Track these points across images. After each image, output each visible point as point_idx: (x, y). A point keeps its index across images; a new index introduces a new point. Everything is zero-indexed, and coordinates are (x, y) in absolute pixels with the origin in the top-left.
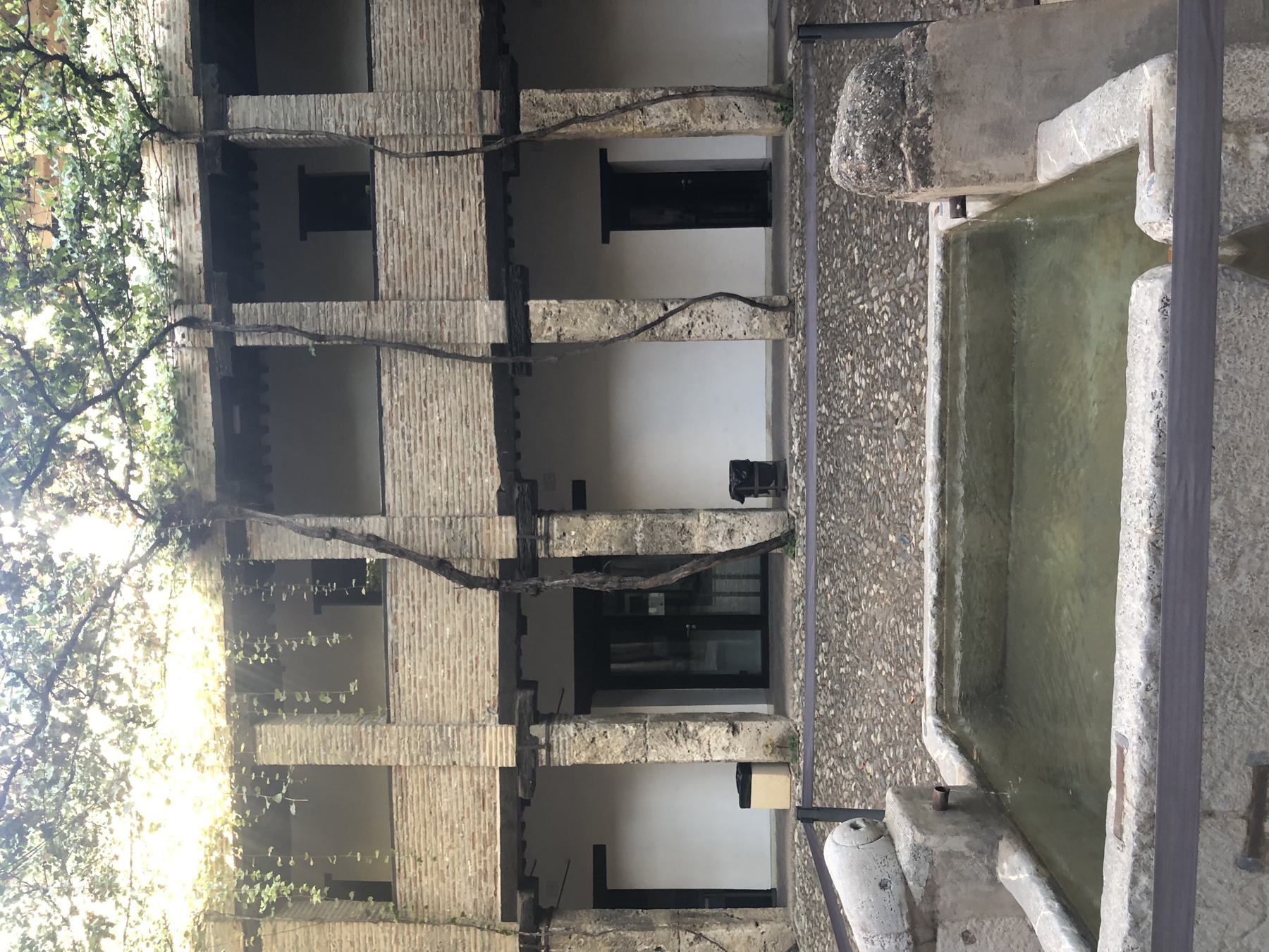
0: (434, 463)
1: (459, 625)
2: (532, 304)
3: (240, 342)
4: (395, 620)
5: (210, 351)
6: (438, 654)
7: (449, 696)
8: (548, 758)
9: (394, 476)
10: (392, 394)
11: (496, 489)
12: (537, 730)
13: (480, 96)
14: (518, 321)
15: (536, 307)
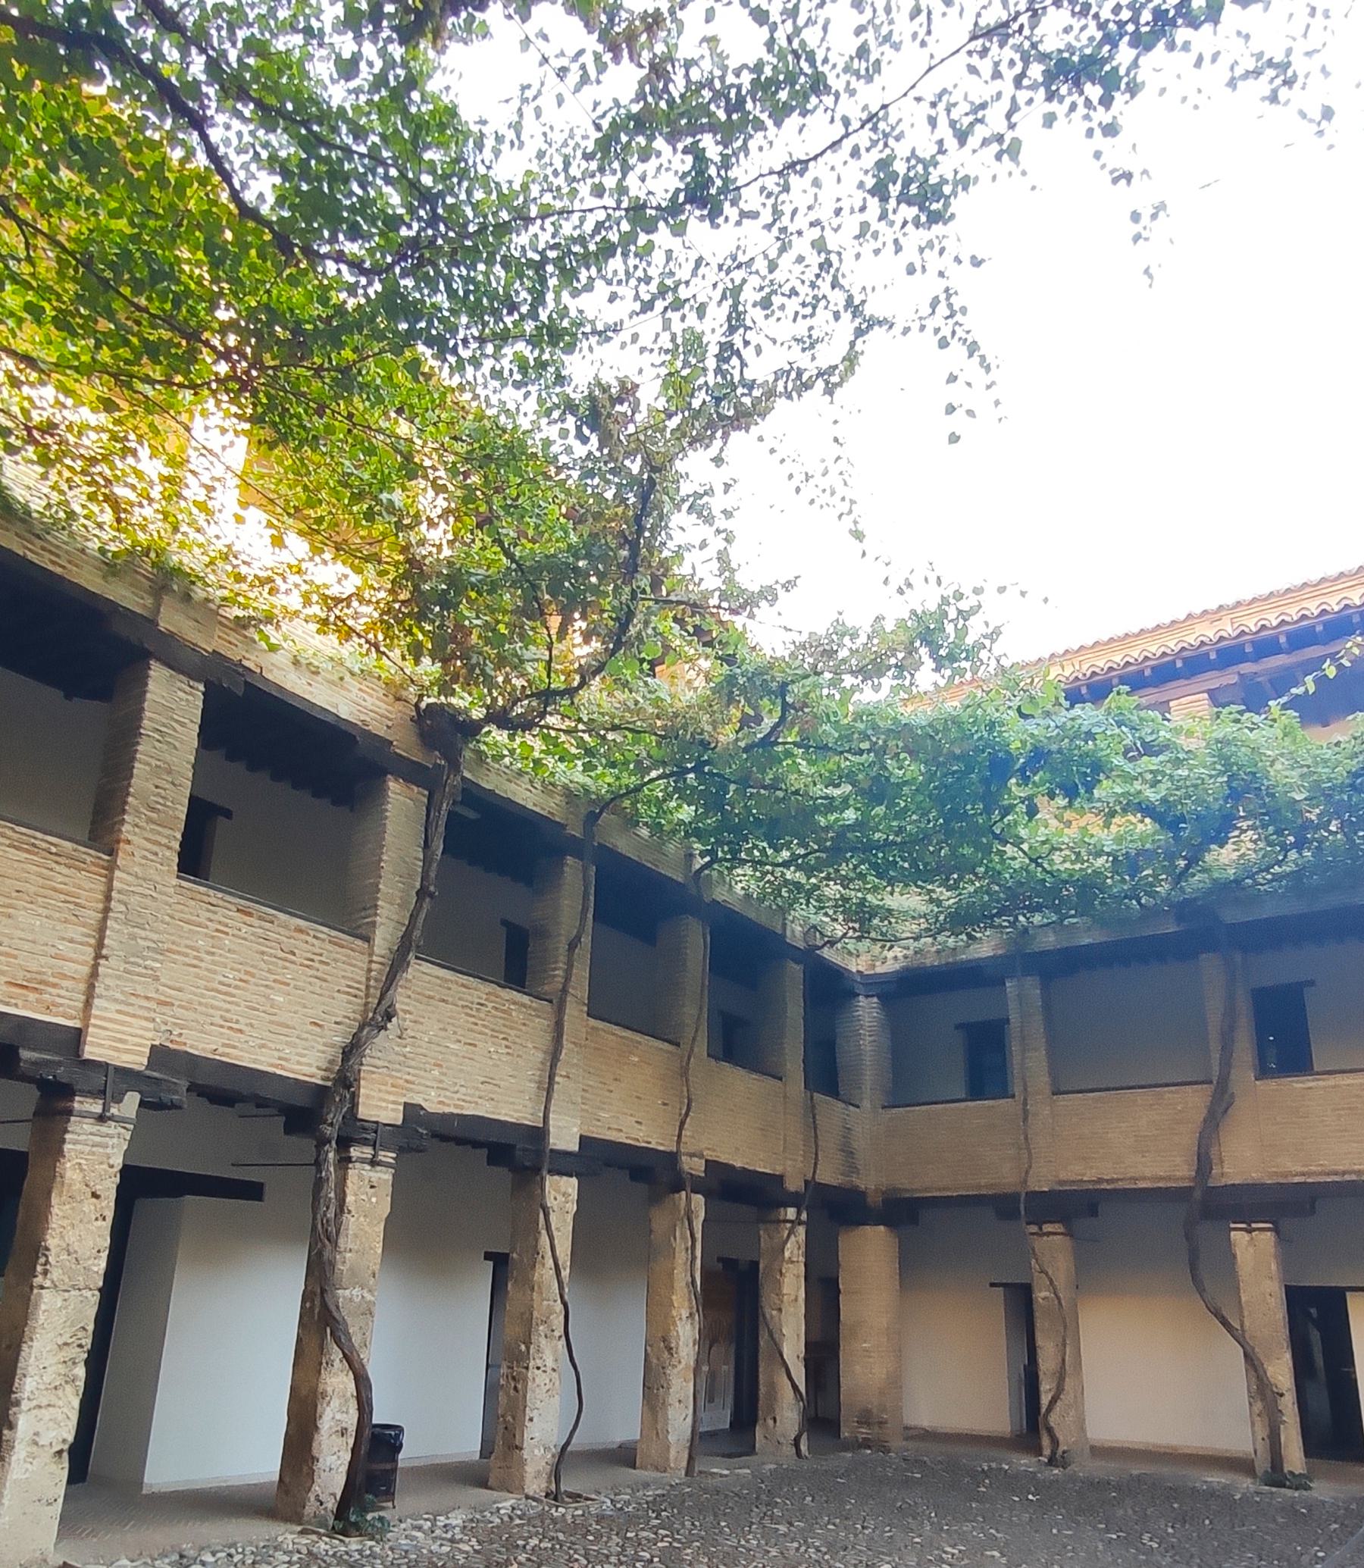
0: (455, 1033)
1: (284, 1017)
2: (574, 1181)
3: (569, 860)
4: (300, 931)
5: (563, 826)
6: (253, 975)
7: (197, 976)
8: (84, 1115)
9: (447, 981)
10: (514, 1003)
11: (424, 1105)
12: (131, 1103)
13: (701, 1156)
14: (563, 1163)
15: (570, 1185)
